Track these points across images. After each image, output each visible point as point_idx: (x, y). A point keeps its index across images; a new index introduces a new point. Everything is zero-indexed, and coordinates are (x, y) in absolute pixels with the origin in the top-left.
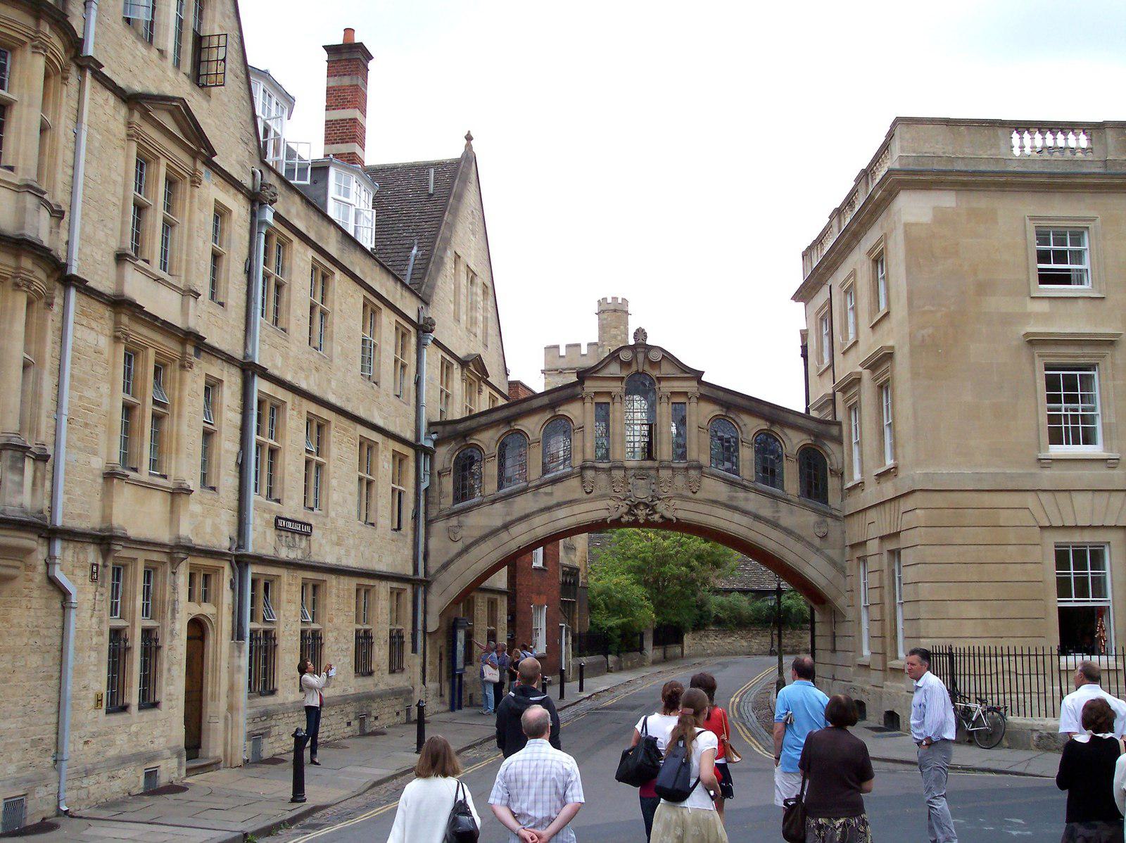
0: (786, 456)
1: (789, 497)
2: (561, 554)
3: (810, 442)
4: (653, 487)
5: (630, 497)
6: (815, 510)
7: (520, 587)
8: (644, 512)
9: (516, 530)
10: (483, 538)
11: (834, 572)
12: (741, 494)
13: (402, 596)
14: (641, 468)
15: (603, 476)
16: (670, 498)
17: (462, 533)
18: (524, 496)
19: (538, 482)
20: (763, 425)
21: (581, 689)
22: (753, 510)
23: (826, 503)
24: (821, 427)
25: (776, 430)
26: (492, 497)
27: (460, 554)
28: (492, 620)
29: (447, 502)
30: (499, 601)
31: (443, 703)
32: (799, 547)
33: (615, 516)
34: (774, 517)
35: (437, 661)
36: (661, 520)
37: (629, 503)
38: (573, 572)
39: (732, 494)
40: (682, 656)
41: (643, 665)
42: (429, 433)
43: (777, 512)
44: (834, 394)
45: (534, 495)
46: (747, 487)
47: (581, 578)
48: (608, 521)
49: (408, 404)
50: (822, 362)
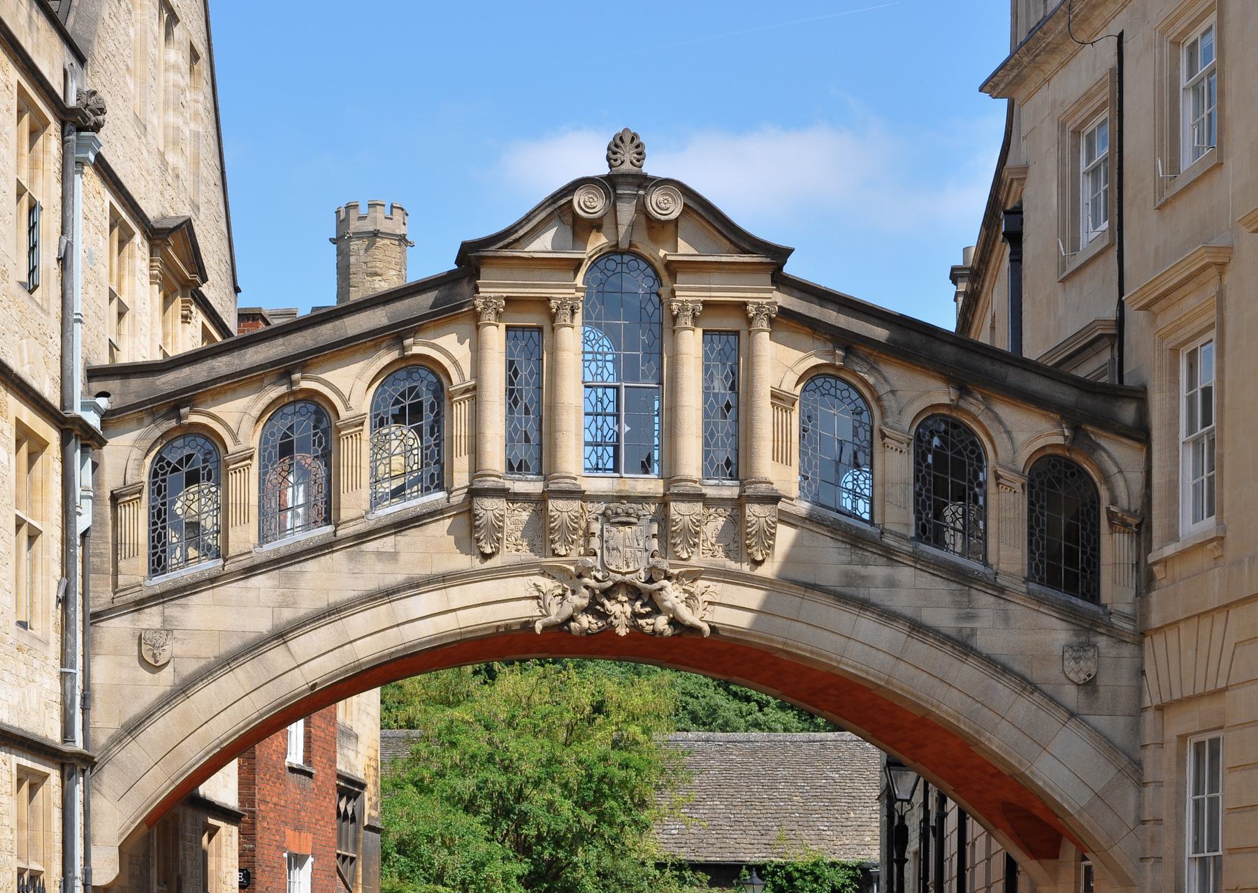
0: (998, 477)
3: (1060, 440)
6: (1069, 614)
8: (628, 609)
11: (1112, 772)
12: (878, 571)
15: (523, 515)
16: (694, 576)
17: (172, 648)
18: (325, 561)
19: (360, 527)
20: (941, 394)
22: (908, 612)
23: (1093, 595)
24: (1089, 402)
25: (973, 409)
26: (246, 562)
29: (135, 569)
32: (1023, 707)
34: (961, 629)
36: (669, 631)
37: (592, 583)
39: (857, 568)
42: (87, 392)
43: (970, 617)
45: (351, 558)
48: (538, 627)
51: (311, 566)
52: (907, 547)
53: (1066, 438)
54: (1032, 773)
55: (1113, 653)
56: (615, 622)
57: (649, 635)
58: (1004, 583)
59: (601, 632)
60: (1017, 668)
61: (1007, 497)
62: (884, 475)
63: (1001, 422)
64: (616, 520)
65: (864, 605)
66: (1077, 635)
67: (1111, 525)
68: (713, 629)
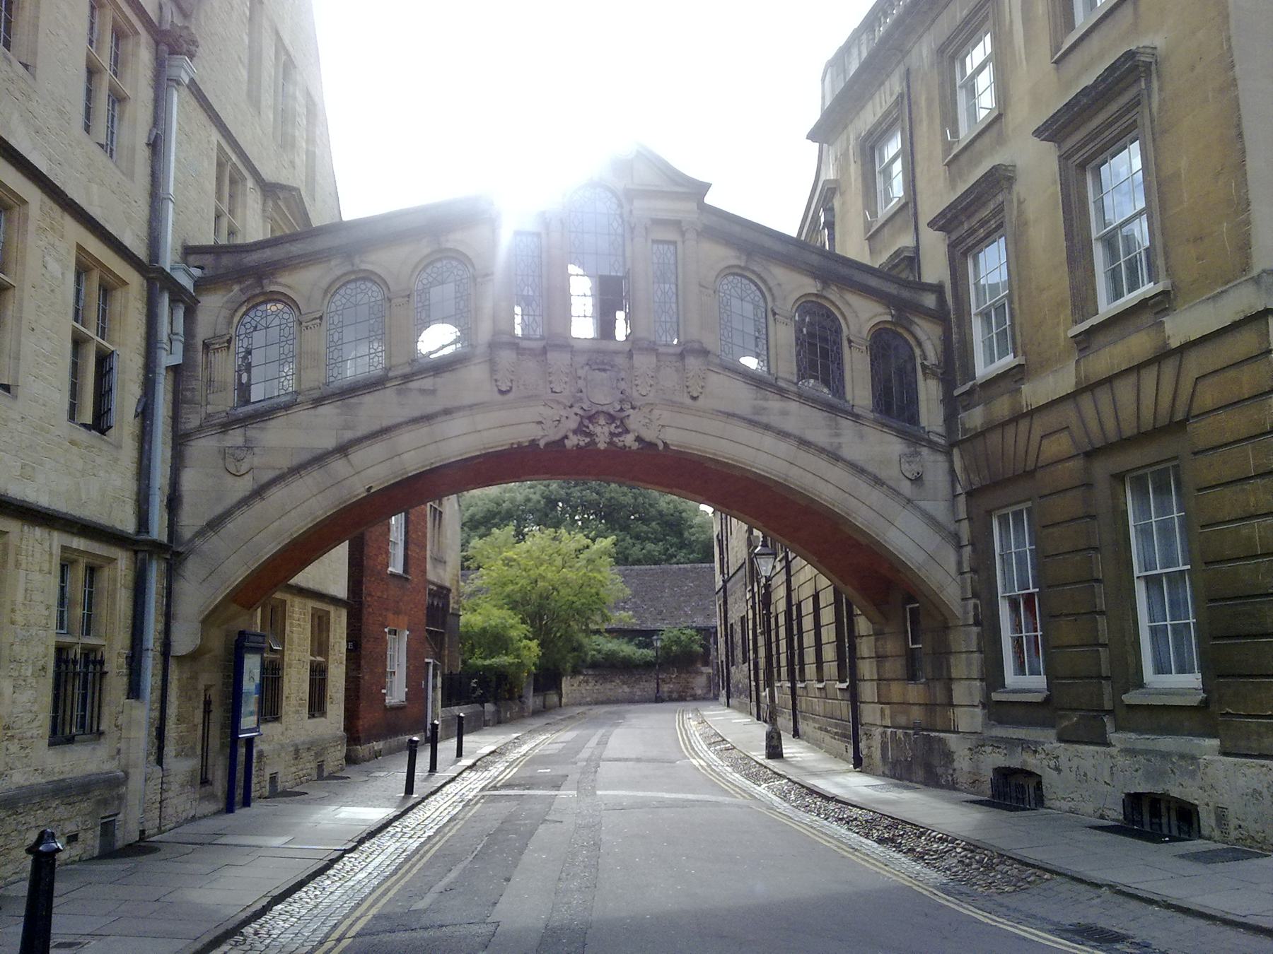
0: (850, 341)
1: (856, 410)
2: (429, 566)
3: (889, 318)
4: (623, 385)
5: (581, 399)
6: (902, 434)
7: (369, 599)
8: (606, 429)
9: (359, 456)
10: (296, 470)
12: (775, 404)
13: (106, 573)
14: (598, 352)
19: (407, 370)
20: (810, 286)
21: (459, 753)
22: (796, 432)
25: (832, 297)
26: (316, 394)
27: (246, 501)
28: (320, 645)
30: (332, 615)
31: (211, 797)
32: (876, 496)
33: (554, 435)
34: (831, 444)
35: (198, 716)
36: (635, 446)
37: (581, 412)
38: (442, 592)
40: (560, 706)
41: (523, 717)
43: (837, 435)
44: (917, 248)
45: (399, 393)
46: (787, 391)
47: (451, 601)
48: (542, 444)
49: (130, 175)
50: (874, 214)
51: (368, 399)
52: (793, 388)
53: (892, 316)
54: (885, 541)
55: (932, 458)
56: (597, 440)
57: (621, 448)
58: (860, 413)
59: (588, 444)
60: (870, 469)
61: (856, 354)
62: (776, 340)
63: (849, 305)
64: (596, 367)
65: (767, 427)
66: (909, 447)
67: (925, 374)
68: (665, 444)
